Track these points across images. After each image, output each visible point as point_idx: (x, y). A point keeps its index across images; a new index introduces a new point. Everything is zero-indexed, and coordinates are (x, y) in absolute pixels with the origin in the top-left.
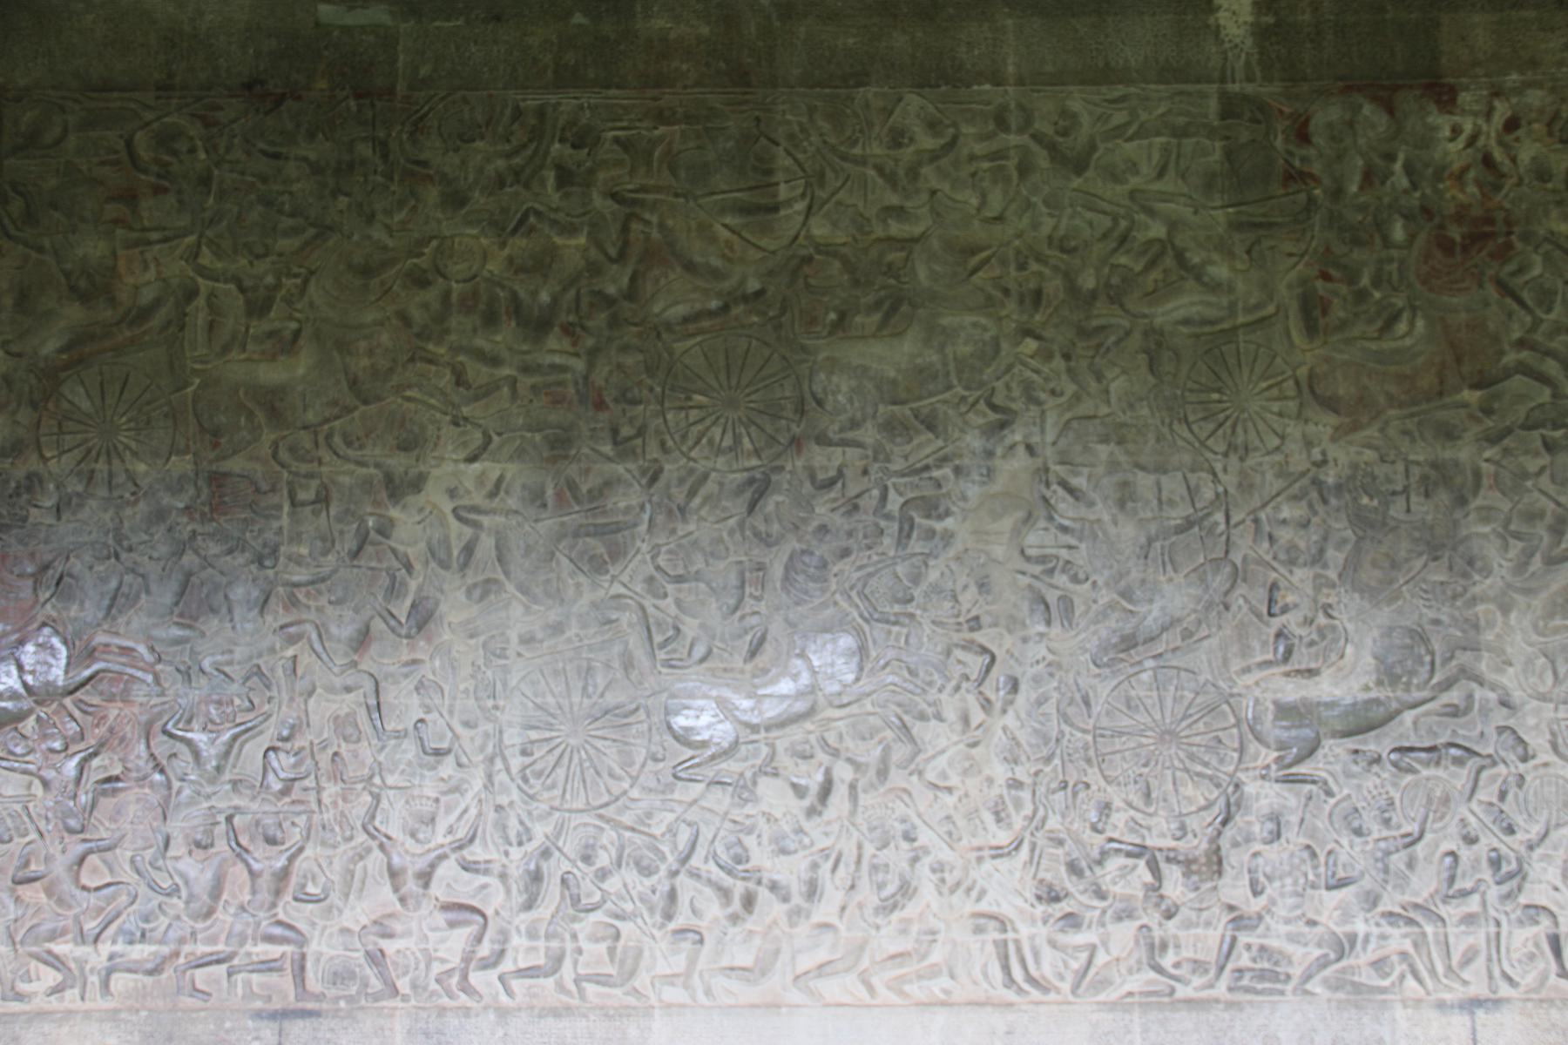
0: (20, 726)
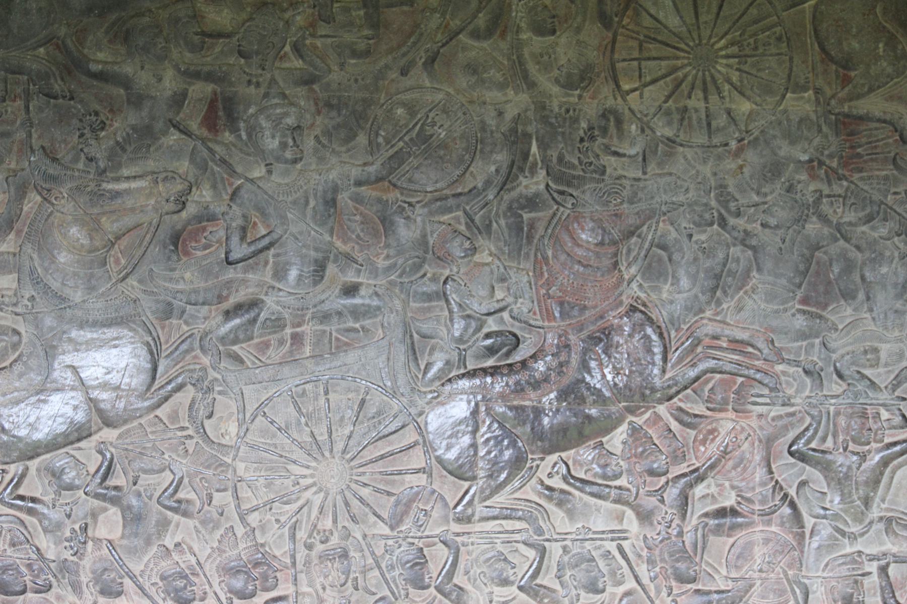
0: (604, 440)
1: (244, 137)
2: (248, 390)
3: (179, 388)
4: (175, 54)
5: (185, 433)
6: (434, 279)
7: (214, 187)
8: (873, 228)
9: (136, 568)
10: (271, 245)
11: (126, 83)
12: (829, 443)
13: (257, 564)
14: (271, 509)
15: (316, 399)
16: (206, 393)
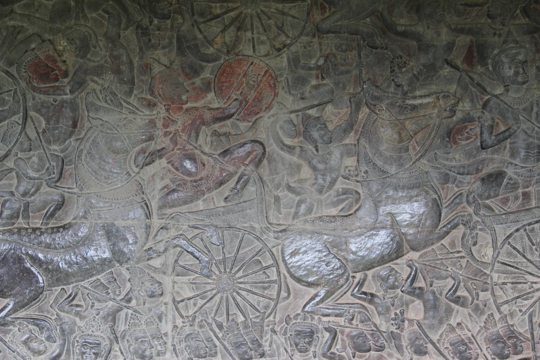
1: (491, 69)
2: (498, 228)
3: (455, 226)
5: (459, 255)
7: (472, 101)
9: (435, 338)
10: (510, 136)
11: (418, 38)
13: (510, 338)
14: (516, 303)
16: (472, 230)
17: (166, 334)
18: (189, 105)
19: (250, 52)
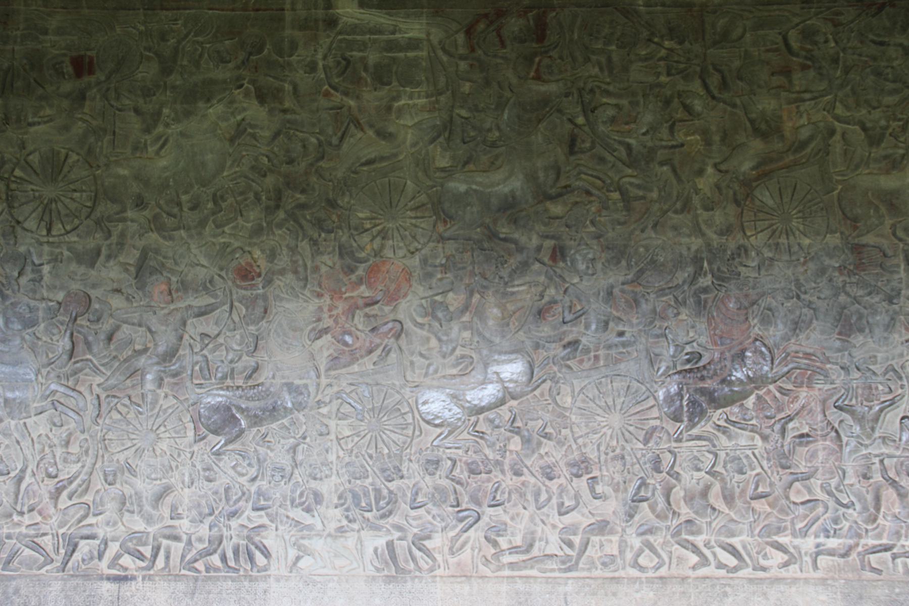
0: (744, 402)
1: (569, 264)
2: (575, 382)
3: (544, 381)
4: (537, 228)
6: (660, 328)
7: (556, 288)
8: (872, 298)
9: (529, 463)
11: (515, 242)
12: (854, 402)
13: (583, 462)
15: (607, 385)
17: (332, 463)
18: (347, 295)
19: (392, 255)
